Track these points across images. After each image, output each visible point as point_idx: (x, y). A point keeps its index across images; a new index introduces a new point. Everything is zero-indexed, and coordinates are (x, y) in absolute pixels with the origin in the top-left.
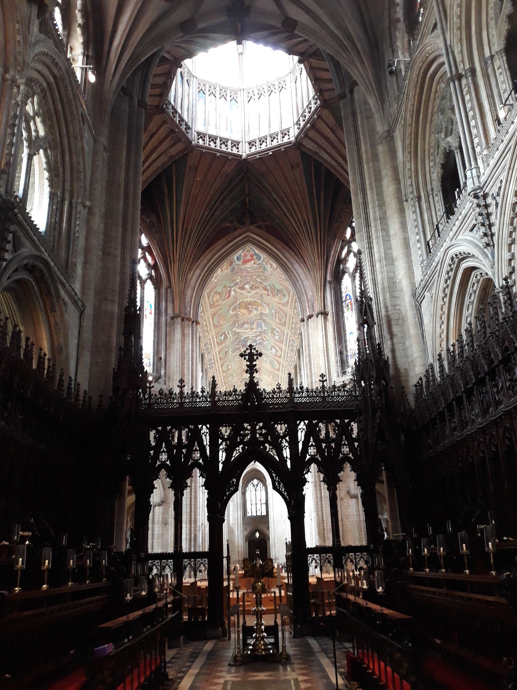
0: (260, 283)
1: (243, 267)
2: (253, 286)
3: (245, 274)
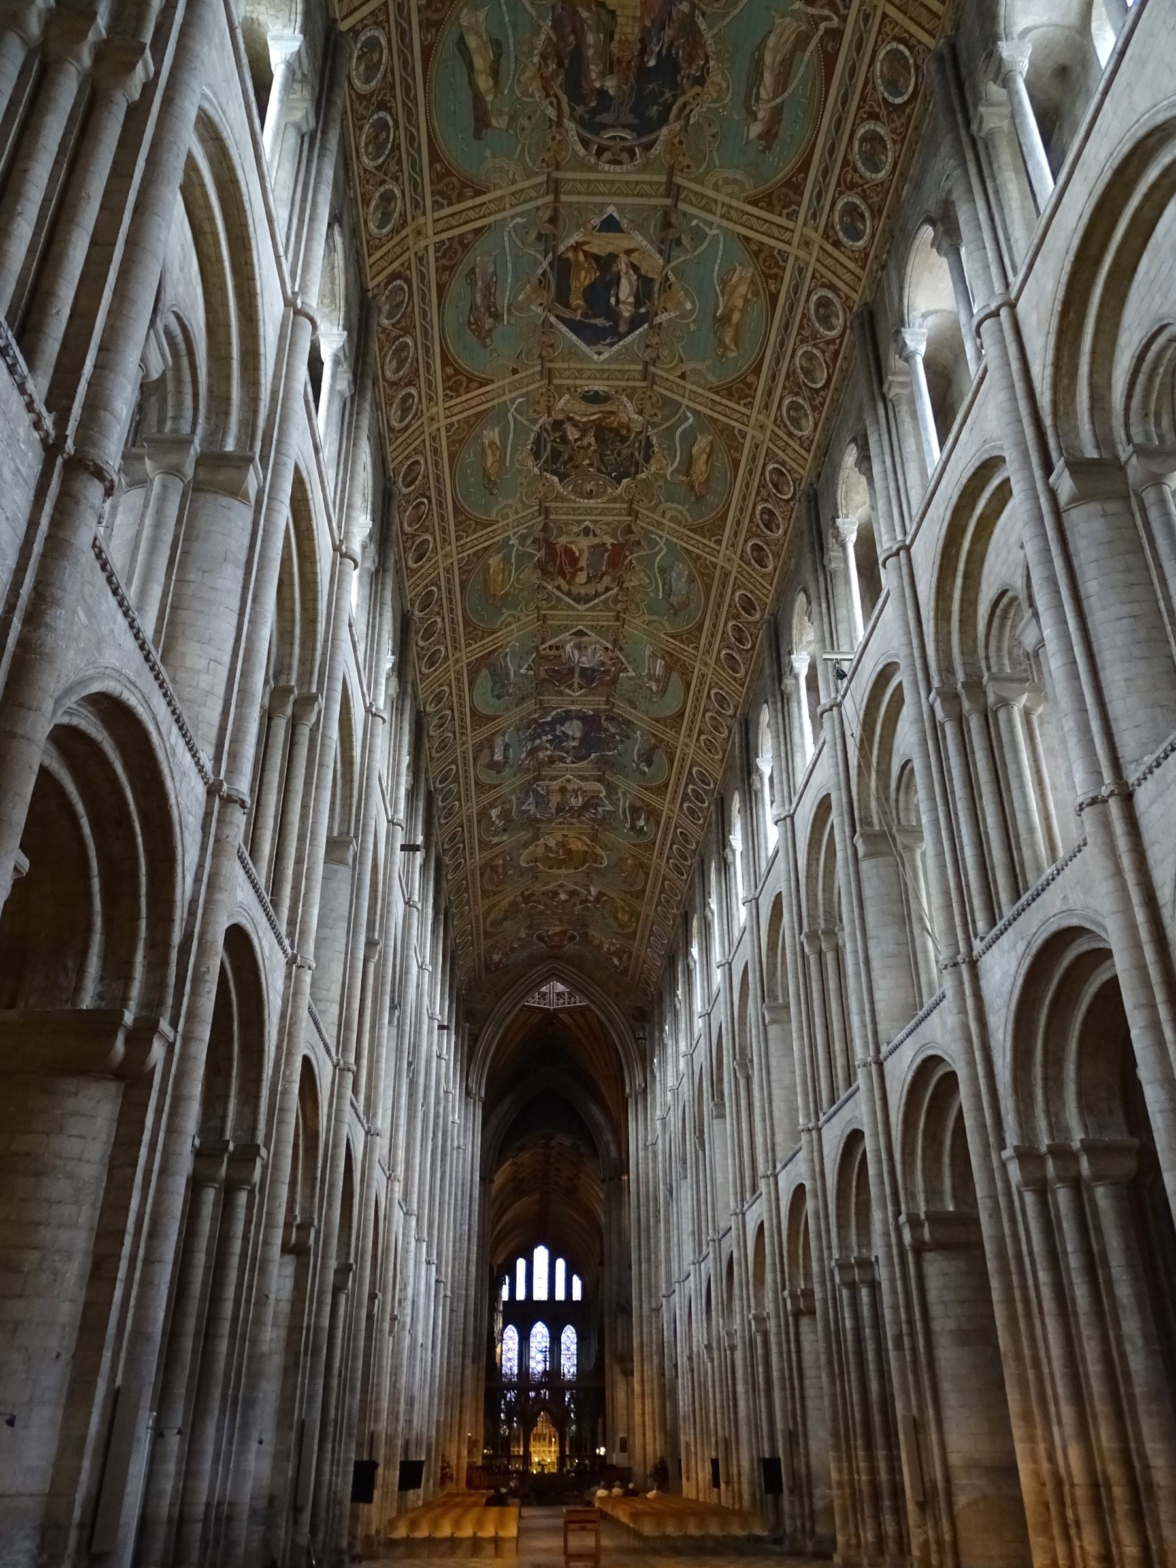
1: (566, 926)
2: (553, 898)
3: (565, 918)
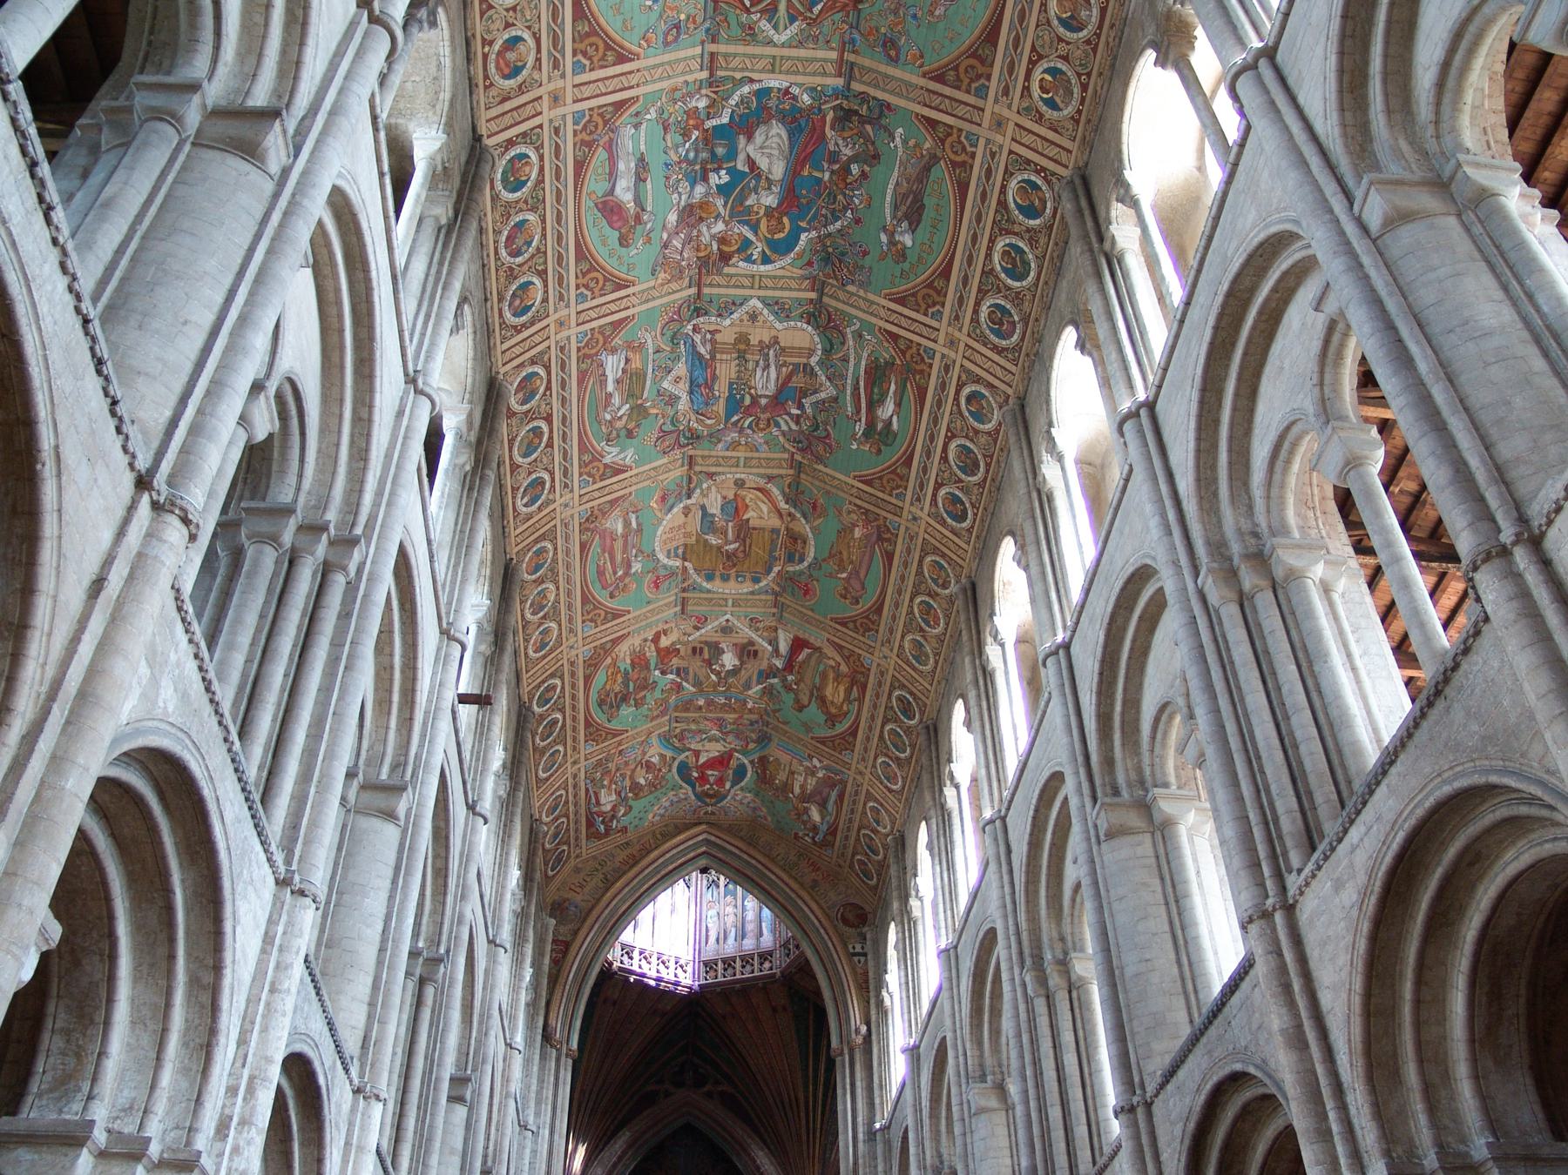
0: (686, 670)
1: (733, 742)
2: (711, 665)
3: (731, 717)
